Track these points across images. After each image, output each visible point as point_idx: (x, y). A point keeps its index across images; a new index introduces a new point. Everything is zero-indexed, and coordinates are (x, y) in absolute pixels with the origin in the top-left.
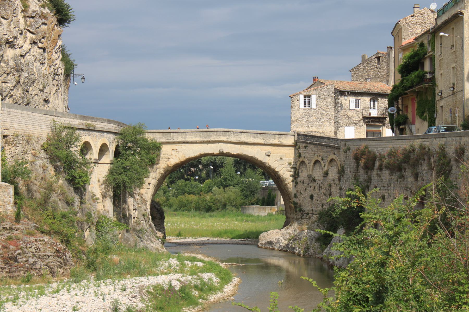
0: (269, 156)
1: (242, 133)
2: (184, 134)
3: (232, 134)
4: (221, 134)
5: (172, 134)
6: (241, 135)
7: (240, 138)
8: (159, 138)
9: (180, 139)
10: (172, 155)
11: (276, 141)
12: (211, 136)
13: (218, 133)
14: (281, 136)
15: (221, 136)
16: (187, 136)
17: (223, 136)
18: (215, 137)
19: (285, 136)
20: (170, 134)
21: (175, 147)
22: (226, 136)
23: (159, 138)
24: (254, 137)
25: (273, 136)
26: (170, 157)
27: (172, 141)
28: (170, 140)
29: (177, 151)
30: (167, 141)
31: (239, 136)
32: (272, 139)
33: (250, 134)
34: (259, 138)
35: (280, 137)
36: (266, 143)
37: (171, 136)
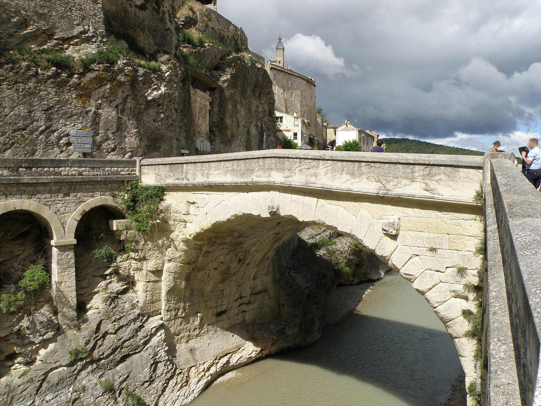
0: (394, 237)
1: (321, 162)
2: (207, 164)
4: (273, 166)
5: (185, 165)
6: (317, 167)
7: (316, 175)
9: (200, 179)
10: (188, 214)
12: (252, 171)
14: (435, 169)
15: (271, 169)
16: (212, 172)
17: (277, 170)
18: (260, 173)
19: (449, 169)
20: (182, 168)
21: (191, 196)
22: (283, 170)
24: (353, 174)
25: (409, 169)
26: (186, 218)
27: (185, 182)
28: (183, 179)
29: (196, 204)
31: (312, 171)
32: (404, 181)
33: (339, 164)
34: (364, 177)
36: (381, 193)
37: (184, 171)
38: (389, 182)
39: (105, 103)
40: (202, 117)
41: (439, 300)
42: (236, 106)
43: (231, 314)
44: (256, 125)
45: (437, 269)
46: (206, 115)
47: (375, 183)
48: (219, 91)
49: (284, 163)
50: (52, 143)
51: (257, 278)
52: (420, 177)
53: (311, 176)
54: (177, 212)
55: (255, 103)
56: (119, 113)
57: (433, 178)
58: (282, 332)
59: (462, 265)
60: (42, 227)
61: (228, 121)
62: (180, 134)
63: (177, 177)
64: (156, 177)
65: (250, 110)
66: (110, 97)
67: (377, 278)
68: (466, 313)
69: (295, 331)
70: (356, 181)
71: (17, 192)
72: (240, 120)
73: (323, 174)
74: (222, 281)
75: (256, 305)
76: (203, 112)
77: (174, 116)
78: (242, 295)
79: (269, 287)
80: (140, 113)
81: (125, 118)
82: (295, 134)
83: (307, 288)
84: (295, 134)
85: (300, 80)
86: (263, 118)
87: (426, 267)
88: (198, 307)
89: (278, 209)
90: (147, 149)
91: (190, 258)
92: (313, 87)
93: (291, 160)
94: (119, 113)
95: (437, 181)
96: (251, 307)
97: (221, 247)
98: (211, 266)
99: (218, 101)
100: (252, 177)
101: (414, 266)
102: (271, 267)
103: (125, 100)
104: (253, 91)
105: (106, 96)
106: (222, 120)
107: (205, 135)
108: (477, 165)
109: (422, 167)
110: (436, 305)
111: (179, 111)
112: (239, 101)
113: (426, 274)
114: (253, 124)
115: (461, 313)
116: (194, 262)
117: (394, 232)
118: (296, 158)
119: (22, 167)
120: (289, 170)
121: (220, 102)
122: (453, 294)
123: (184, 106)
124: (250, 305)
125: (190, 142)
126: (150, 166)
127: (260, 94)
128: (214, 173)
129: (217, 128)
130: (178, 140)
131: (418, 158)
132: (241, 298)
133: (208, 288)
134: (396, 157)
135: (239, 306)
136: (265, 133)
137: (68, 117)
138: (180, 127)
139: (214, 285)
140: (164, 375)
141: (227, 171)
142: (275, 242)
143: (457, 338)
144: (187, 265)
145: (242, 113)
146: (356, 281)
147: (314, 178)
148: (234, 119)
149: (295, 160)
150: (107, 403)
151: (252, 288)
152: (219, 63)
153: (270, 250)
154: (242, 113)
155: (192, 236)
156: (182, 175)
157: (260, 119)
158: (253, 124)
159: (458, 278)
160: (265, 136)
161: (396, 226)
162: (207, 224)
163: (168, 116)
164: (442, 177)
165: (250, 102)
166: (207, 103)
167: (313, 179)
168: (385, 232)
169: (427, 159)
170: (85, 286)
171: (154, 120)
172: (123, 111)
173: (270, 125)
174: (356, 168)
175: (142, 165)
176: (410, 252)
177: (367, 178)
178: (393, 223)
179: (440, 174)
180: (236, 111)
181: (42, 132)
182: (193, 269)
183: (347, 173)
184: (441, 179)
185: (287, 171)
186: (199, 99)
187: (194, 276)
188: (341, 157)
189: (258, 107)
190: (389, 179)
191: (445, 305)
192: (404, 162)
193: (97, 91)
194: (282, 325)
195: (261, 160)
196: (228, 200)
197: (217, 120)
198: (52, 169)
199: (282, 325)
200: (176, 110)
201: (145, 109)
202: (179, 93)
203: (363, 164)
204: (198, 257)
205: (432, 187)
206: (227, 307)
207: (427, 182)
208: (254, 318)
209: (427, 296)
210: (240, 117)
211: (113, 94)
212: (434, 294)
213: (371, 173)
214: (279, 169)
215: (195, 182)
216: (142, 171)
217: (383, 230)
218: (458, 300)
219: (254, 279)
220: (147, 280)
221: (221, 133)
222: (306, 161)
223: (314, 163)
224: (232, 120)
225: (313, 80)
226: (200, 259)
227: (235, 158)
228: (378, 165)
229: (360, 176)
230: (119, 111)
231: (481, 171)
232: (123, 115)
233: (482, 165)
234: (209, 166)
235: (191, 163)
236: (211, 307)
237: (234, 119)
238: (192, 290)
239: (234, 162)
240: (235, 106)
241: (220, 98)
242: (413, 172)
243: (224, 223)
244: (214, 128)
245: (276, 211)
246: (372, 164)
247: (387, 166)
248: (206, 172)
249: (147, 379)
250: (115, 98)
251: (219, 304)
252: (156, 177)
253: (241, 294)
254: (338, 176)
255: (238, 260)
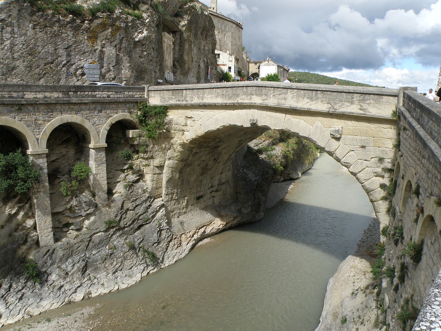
0: (338, 139)
1: (289, 90)
2: (202, 90)
3: (272, 92)
4: (254, 92)
5: (184, 91)
7: (285, 99)
8: (168, 98)
9: (196, 101)
11: (354, 109)
12: (238, 95)
13: (249, 89)
14: (367, 97)
15: (253, 94)
16: (205, 96)
17: (257, 95)
18: (244, 97)
19: (376, 96)
20: (182, 93)
21: (189, 113)
22: (261, 95)
23: (168, 98)
24: (311, 99)
25: (349, 96)
26: (184, 128)
27: (184, 103)
28: (183, 101)
29: (193, 119)
30: (178, 102)
32: (346, 104)
33: (302, 92)
35: (364, 100)
36: (331, 111)
37: (184, 95)
38: (336, 104)
39: (108, 43)
40: (168, 54)
41: (366, 178)
42: (191, 46)
43: (205, 198)
44: (204, 60)
45: (365, 159)
46: (170, 53)
47: (326, 105)
48: (179, 33)
49: (262, 90)
50: (72, 74)
51: (223, 173)
52: (357, 101)
53: (282, 99)
54: (177, 124)
55: (203, 43)
56: (117, 51)
57: (365, 102)
58: (239, 211)
59: (381, 156)
60: (79, 135)
61: (186, 58)
62: (156, 67)
63: (178, 99)
64: (161, 99)
65: (199, 49)
66: (111, 38)
67: (296, 177)
68: (383, 186)
69: (248, 211)
70: (313, 103)
71: (68, 109)
72: (193, 56)
73: (290, 98)
74: (202, 174)
75: (221, 192)
76: (169, 50)
77: (152, 54)
78: (213, 185)
79: (230, 180)
80: (131, 51)
81: (121, 55)
82: (230, 68)
83: (255, 180)
84: (230, 68)
85: (231, 23)
86: (208, 54)
87: (359, 158)
88: (186, 192)
89: (257, 121)
90: (136, 79)
91: (184, 157)
92: (240, 29)
93: (267, 88)
94: (117, 51)
95: (368, 104)
96: (218, 193)
97: (205, 149)
98: (196, 163)
99: (179, 41)
100: (238, 100)
101: (350, 157)
102: (232, 166)
103: (121, 41)
104: (202, 34)
105: (108, 38)
106: (181, 56)
107: (170, 68)
108: (394, 94)
109: (359, 95)
110: (363, 182)
111: (155, 49)
112: (193, 41)
113: (358, 162)
114: (202, 60)
115: (379, 186)
116: (186, 160)
117: (339, 136)
118: (271, 87)
119: (71, 91)
120: (265, 95)
121: (181, 42)
122: (375, 174)
123: (159, 45)
124: (218, 192)
125: (162, 73)
126: (156, 92)
127: (206, 36)
128: (208, 97)
129: (178, 63)
130: (155, 72)
131: (356, 89)
132: (212, 187)
133: (193, 179)
134: (342, 88)
135: (211, 193)
136: (209, 67)
137: (82, 54)
138: (156, 62)
139: (196, 177)
140: (166, 239)
141: (218, 95)
142: (238, 147)
143: (375, 201)
144: (181, 162)
145: (195, 51)
146: (282, 179)
147: (284, 100)
148: (190, 56)
149: (270, 88)
150: (132, 256)
151: (220, 180)
152: (178, 11)
153: (233, 153)
154: (195, 51)
155: (189, 141)
156: (182, 97)
157: (206, 56)
158: (202, 60)
159: (379, 164)
160: (209, 69)
161: (340, 132)
162: (201, 132)
163: (148, 53)
164: (372, 101)
165: (200, 42)
166: (172, 43)
167: (283, 101)
168: (332, 136)
169: (362, 90)
170: (111, 177)
171: (140, 57)
172: (120, 49)
173: (213, 61)
174: (314, 95)
175: (150, 91)
176: (349, 149)
177: (321, 101)
178: (338, 130)
179: (370, 100)
180: (191, 50)
181: (64, 66)
182: (185, 165)
183: (308, 98)
184: (370, 103)
185: (264, 96)
186: (166, 40)
187: (184, 170)
188: (303, 87)
189: (205, 46)
190: (336, 102)
191: (369, 181)
192: (347, 91)
193: (102, 34)
194: (239, 206)
195: (245, 88)
196: (218, 115)
197: (178, 56)
198: (90, 93)
199: (239, 206)
200: (153, 49)
201: (133, 48)
202: (155, 35)
203: (319, 92)
204: (189, 156)
205: (364, 107)
206: (204, 193)
207: (362, 104)
208: (220, 202)
209: (358, 176)
210: (193, 54)
211: (112, 36)
212: (362, 175)
213: (324, 98)
214: (258, 95)
215: (192, 102)
216: (149, 95)
217: (331, 134)
218: (378, 178)
219: (221, 173)
220: (154, 173)
221: (181, 67)
222: (278, 89)
223: (284, 91)
224: (188, 56)
225: (241, 24)
226: (190, 158)
227: (224, 86)
228: (329, 93)
229: (316, 100)
230: (117, 49)
231: (396, 98)
232: (120, 53)
233: (397, 95)
234: (203, 92)
235: (189, 89)
236: (193, 193)
237: (190, 56)
238: (183, 180)
239: (224, 89)
240: (190, 46)
241: (180, 39)
242: (353, 98)
243: (214, 131)
244: (176, 63)
245: (255, 123)
246: (325, 92)
247: (335, 93)
248: (201, 95)
249: (156, 241)
250: (114, 39)
251: (199, 190)
252: (161, 99)
253: (212, 184)
254: (301, 99)
255: (213, 159)
